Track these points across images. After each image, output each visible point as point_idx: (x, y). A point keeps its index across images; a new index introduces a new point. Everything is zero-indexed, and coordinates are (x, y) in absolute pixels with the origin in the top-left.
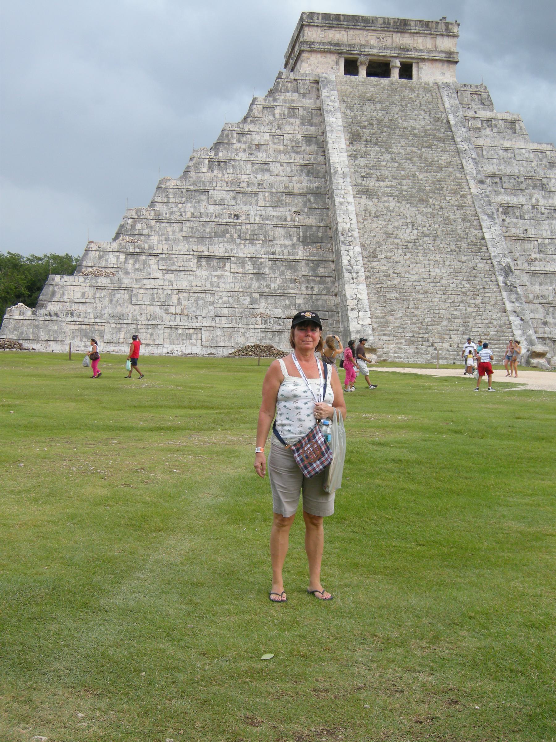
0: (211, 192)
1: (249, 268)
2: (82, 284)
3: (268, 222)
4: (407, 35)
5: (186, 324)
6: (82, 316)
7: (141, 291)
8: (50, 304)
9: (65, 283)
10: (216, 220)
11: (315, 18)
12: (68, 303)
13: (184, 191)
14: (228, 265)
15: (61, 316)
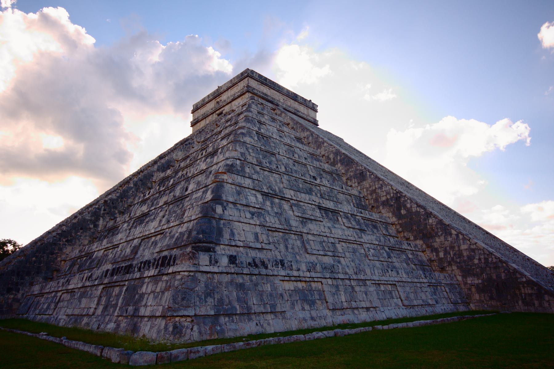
0: (277, 155)
1: (354, 223)
2: (251, 222)
3: (334, 188)
4: (297, 103)
5: (384, 278)
6: (294, 267)
7: (310, 237)
8: (217, 248)
9: (231, 218)
10: (303, 178)
11: (255, 75)
12: (241, 249)
13: (258, 149)
14: (340, 218)
15: (269, 266)
